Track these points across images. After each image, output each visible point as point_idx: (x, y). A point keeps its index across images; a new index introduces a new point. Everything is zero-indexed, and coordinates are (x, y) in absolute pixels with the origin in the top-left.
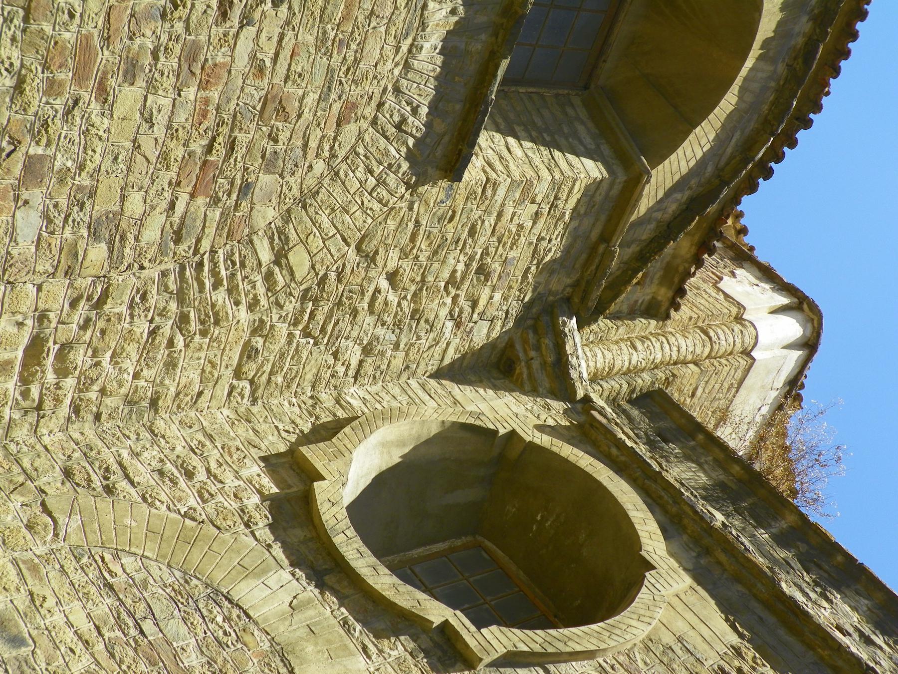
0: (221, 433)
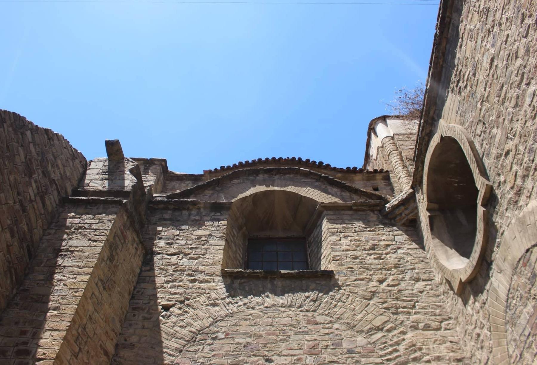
0: (463, 327)
